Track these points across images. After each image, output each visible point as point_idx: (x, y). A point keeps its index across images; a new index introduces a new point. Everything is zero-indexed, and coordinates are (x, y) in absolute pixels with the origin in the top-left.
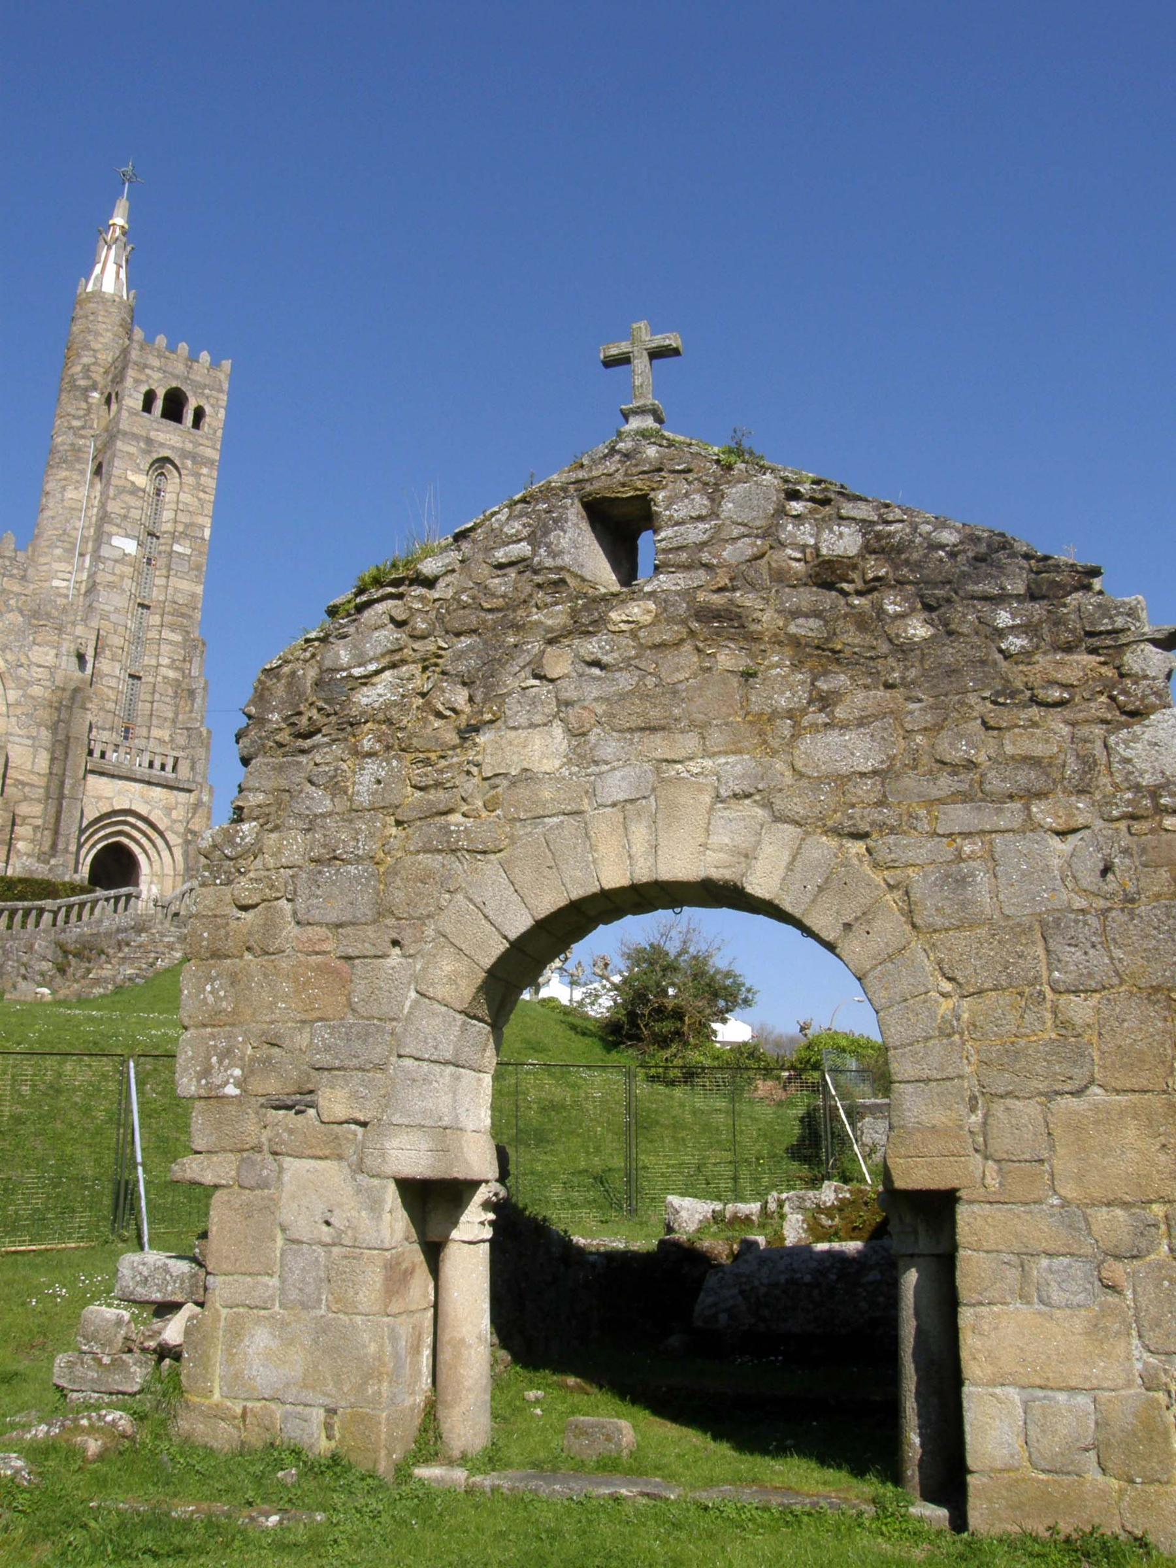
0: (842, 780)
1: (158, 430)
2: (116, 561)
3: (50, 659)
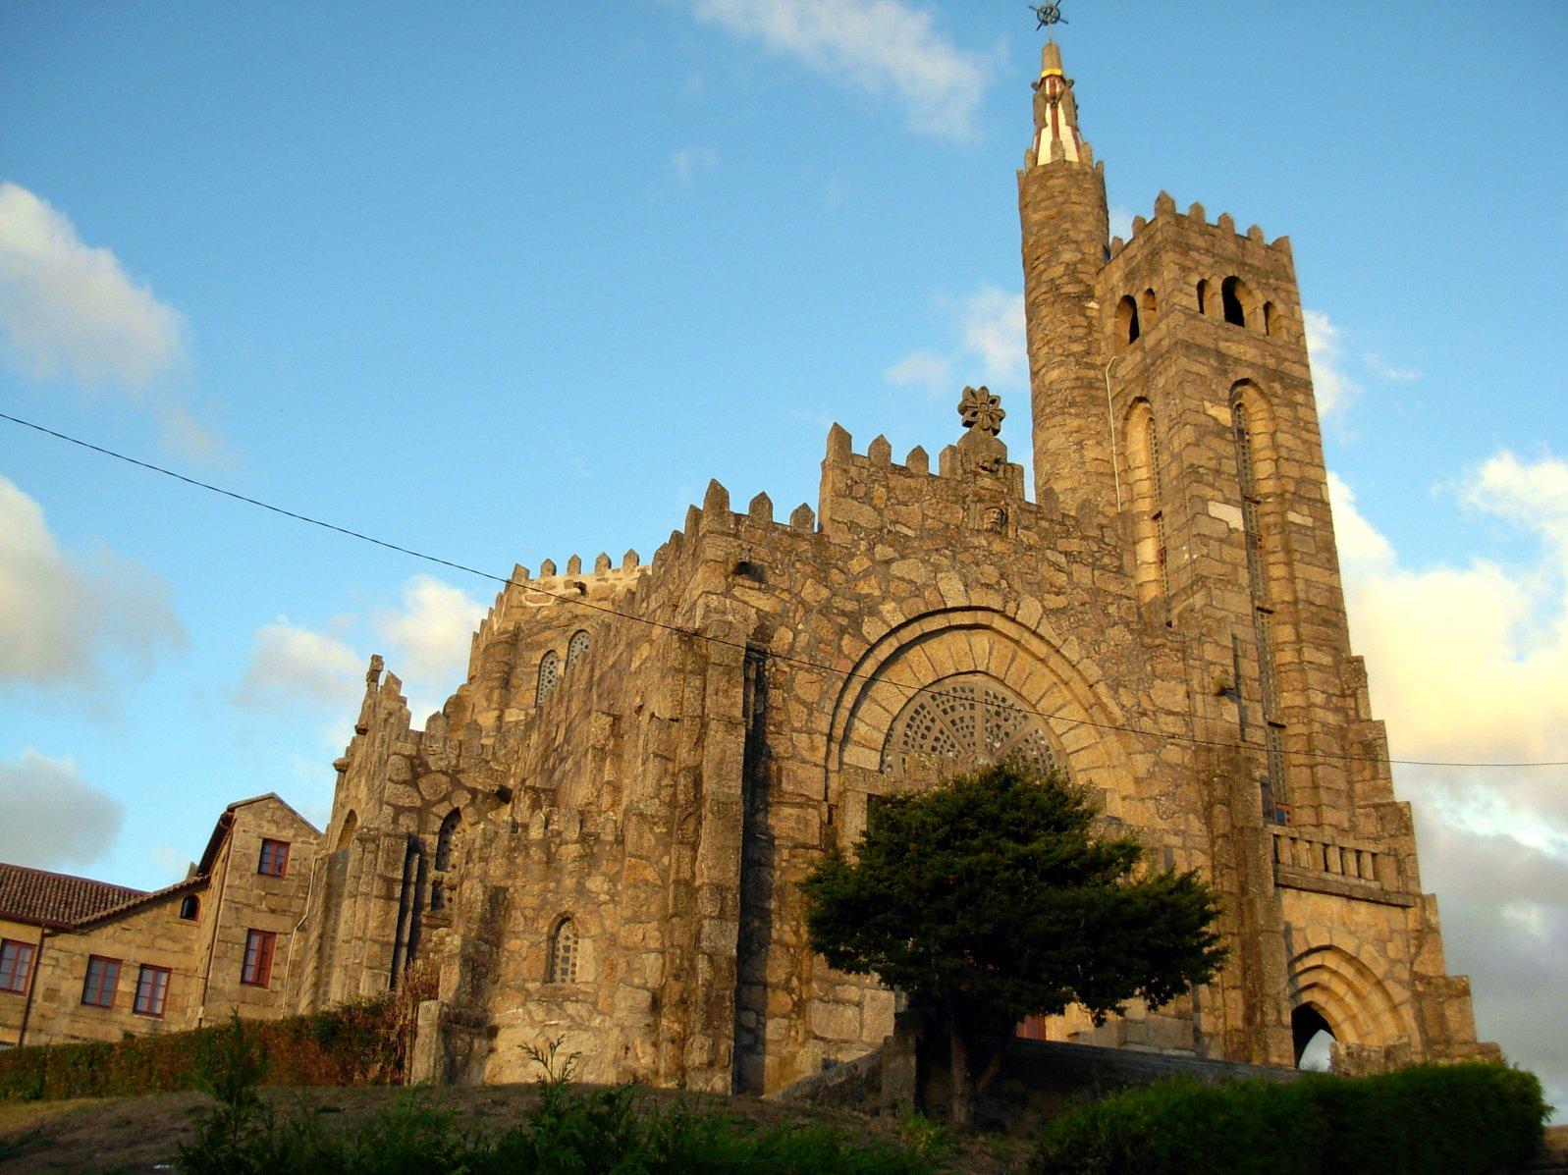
2: (1221, 541)
3: (1179, 702)
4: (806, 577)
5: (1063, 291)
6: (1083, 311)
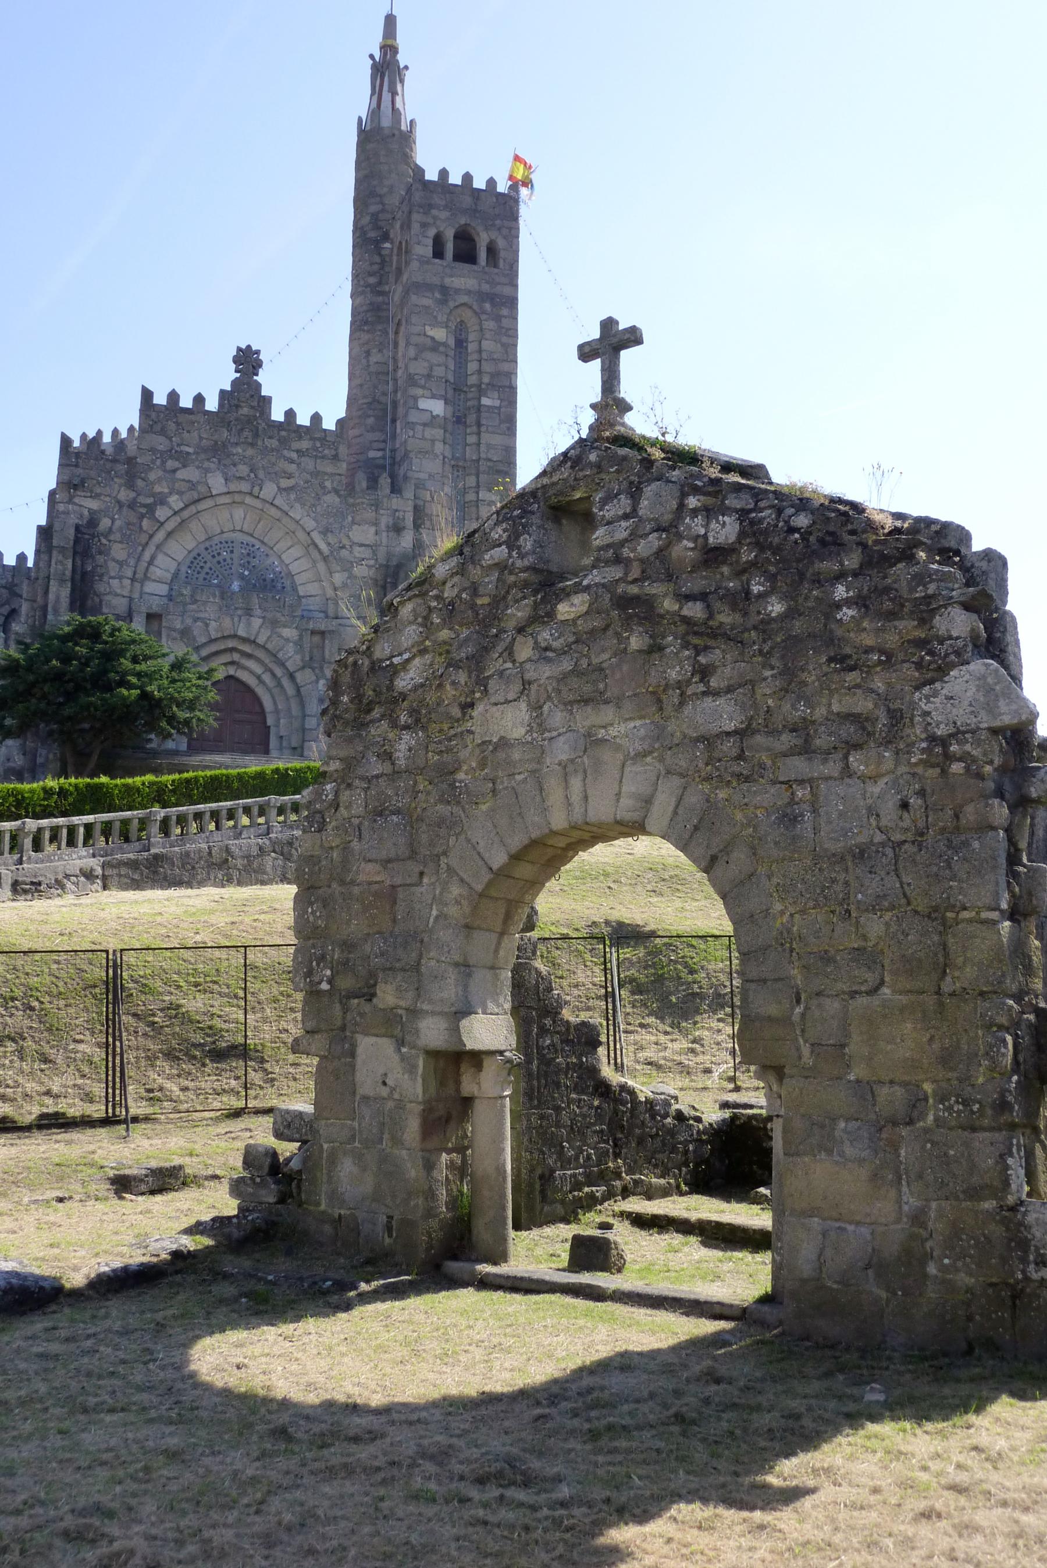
0: (708, 740)
2: (425, 425)
4: (120, 486)
6: (378, 250)
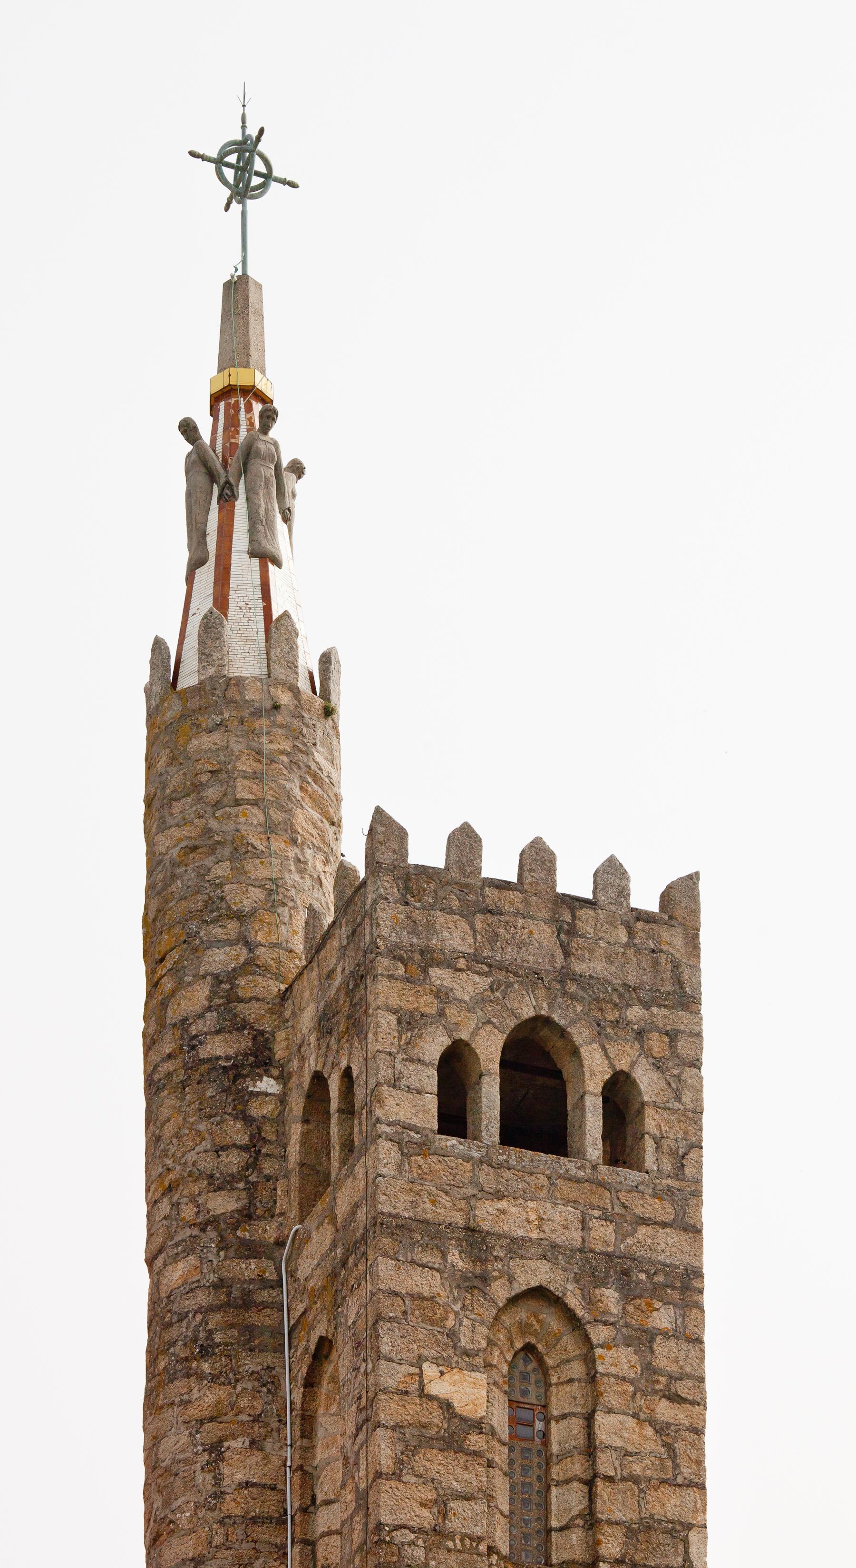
1: (498, 1196)
5: (204, 1052)
6: (241, 1104)
